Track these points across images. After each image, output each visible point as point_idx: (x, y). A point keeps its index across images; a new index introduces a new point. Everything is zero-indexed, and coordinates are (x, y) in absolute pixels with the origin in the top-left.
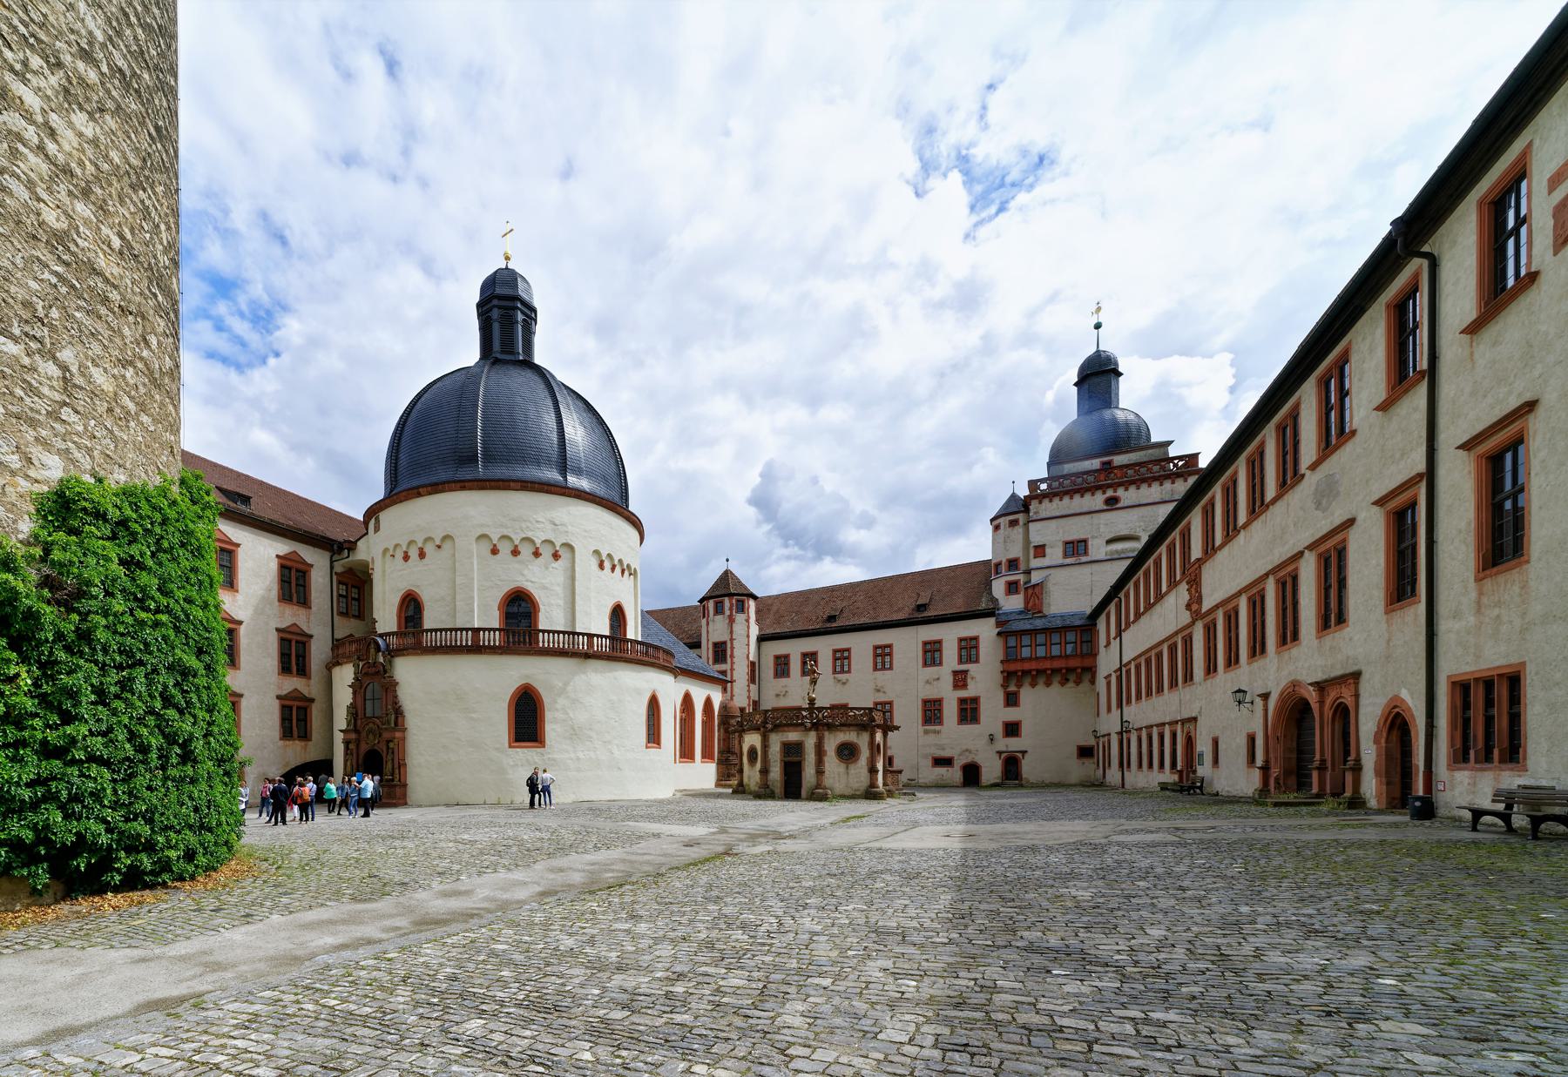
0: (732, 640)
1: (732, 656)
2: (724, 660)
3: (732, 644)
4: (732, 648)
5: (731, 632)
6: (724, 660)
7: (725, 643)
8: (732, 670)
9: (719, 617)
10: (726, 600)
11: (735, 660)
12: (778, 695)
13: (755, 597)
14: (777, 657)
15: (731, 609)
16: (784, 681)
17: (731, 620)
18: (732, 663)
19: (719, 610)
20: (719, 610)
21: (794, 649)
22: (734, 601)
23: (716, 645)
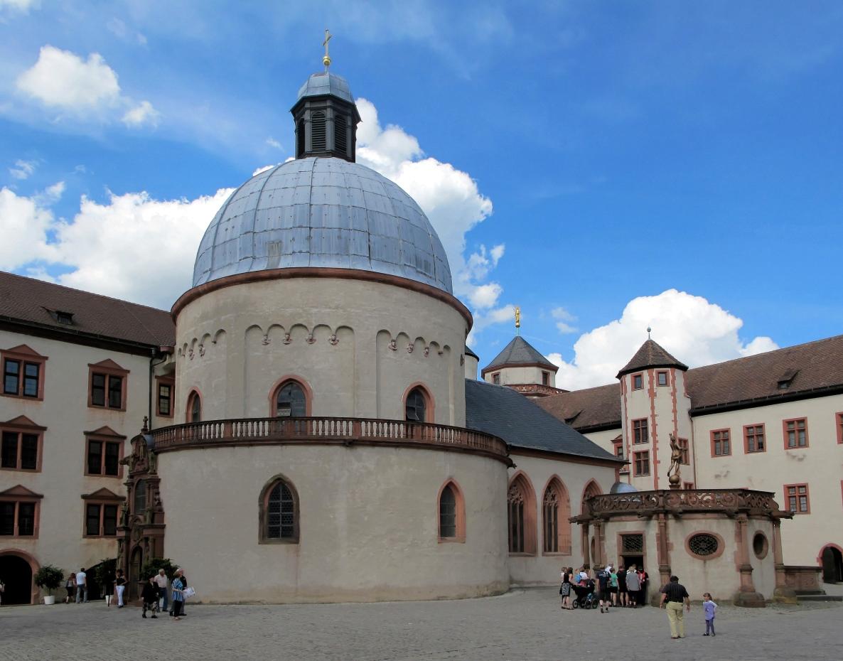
0: (653, 416)
1: (654, 434)
2: (646, 440)
3: (654, 421)
4: (654, 425)
5: (653, 408)
6: (646, 440)
7: (645, 421)
8: (655, 449)
9: (638, 392)
10: (645, 373)
11: (657, 438)
12: (717, 476)
13: (684, 368)
14: (716, 433)
15: (651, 383)
16: (723, 460)
17: (652, 394)
18: (655, 442)
19: (637, 385)
20: (637, 385)
21: (735, 422)
22: (654, 374)
23: (636, 422)
